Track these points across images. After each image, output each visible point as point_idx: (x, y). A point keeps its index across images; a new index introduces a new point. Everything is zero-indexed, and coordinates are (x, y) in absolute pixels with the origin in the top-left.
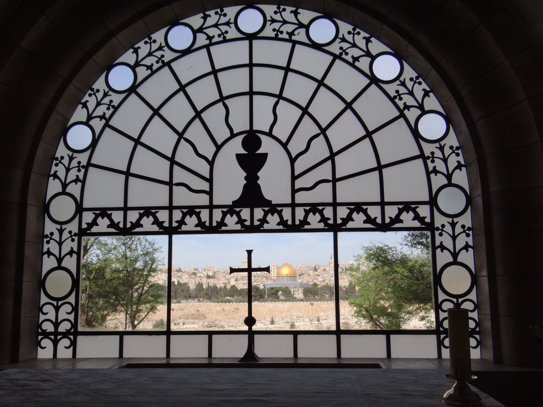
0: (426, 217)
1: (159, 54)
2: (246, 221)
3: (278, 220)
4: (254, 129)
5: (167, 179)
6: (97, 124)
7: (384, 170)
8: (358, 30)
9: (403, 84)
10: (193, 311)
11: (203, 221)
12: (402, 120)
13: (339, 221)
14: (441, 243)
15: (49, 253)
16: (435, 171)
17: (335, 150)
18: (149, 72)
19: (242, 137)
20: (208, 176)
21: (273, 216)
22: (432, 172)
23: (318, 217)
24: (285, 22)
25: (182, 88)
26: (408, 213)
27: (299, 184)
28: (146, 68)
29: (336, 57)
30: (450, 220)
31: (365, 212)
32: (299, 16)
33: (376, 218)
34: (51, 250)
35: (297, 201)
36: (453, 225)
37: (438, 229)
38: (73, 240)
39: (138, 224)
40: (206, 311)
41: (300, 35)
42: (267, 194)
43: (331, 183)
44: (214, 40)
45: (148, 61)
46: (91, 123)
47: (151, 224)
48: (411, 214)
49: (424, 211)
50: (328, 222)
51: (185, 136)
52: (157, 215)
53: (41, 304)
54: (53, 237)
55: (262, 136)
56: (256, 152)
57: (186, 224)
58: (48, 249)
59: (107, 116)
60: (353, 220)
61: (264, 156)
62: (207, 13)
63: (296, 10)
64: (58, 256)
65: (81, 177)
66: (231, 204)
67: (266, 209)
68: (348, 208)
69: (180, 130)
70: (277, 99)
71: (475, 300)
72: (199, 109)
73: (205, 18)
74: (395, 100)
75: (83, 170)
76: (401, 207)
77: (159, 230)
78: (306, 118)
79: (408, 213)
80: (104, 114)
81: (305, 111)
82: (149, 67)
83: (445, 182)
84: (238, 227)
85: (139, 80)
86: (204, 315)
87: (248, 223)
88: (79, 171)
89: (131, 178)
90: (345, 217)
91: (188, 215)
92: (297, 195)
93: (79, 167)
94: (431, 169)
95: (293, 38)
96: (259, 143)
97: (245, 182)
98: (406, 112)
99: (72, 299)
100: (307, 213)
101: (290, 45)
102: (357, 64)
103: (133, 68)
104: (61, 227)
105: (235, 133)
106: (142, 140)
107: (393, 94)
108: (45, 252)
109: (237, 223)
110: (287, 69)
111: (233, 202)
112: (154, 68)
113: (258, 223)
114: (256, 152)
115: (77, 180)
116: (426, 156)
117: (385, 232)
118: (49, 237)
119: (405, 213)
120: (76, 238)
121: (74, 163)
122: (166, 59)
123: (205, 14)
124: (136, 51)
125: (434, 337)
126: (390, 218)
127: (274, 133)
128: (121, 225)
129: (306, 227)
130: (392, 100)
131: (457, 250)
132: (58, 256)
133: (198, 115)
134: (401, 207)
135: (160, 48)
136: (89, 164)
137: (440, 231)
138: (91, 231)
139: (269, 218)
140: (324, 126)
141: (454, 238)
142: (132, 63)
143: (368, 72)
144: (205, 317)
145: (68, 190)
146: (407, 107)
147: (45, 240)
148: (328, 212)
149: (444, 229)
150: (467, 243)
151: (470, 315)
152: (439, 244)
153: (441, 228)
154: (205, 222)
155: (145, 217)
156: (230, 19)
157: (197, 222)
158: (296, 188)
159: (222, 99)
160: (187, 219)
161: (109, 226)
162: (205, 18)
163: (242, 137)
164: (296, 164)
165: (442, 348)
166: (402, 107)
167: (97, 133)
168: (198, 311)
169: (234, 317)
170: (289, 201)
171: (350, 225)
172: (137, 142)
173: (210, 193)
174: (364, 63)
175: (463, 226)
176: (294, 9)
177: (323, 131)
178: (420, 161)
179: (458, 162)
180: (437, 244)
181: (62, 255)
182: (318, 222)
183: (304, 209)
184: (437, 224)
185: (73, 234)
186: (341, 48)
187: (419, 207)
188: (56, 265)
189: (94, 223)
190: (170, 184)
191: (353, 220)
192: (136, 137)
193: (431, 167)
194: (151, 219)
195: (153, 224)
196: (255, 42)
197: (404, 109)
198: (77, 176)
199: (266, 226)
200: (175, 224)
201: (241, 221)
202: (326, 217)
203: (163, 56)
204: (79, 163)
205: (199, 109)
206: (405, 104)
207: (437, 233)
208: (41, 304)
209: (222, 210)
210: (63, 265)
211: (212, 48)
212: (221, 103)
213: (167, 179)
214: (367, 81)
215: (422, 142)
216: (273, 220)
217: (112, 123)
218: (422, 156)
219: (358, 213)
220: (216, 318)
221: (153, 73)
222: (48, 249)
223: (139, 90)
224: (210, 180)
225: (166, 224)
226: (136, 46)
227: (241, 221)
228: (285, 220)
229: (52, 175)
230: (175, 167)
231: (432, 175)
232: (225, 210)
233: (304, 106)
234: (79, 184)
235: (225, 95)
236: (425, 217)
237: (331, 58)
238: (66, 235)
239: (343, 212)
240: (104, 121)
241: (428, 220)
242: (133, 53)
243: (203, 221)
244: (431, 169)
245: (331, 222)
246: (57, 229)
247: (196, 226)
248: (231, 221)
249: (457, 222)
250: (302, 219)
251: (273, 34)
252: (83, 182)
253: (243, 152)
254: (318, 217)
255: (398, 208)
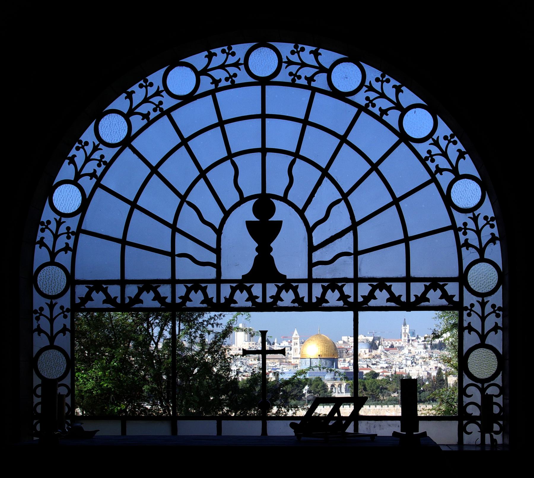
0: (454, 296)
1: (156, 100)
2: (257, 297)
3: (293, 297)
4: (267, 192)
5: (169, 250)
6: (87, 183)
7: (411, 243)
8: (387, 77)
9: (436, 143)
11: (210, 297)
12: (433, 185)
13: (360, 299)
14: (469, 324)
15: (40, 331)
16: (467, 245)
17: (357, 219)
18: (145, 121)
19: (253, 202)
20: (214, 246)
21: (287, 292)
22: (464, 245)
23: (337, 294)
24: (303, 65)
25: (184, 142)
26: (435, 291)
27: (317, 256)
28: (141, 117)
29: (361, 109)
30: (480, 299)
31: (389, 289)
32: (319, 57)
33: (401, 296)
34: (42, 327)
35: (314, 276)
36: (483, 305)
37: (466, 308)
38: (65, 317)
39: (137, 299)
41: (321, 82)
42: (282, 267)
43: (353, 256)
44: (220, 85)
45: (145, 108)
46: (81, 181)
47: (152, 300)
48: (439, 292)
49: (452, 289)
50: (348, 299)
51: (188, 199)
52: (159, 289)
53: (34, 386)
54: (43, 313)
55: (276, 202)
56: (269, 220)
57: (190, 300)
58: (39, 326)
59: (98, 174)
60: (375, 298)
61: (279, 224)
62: (213, 51)
63: (317, 50)
64: (49, 332)
65: (71, 245)
66: (241, 278)
67: (280, 285)
68: (369, 285)
69: (183, 193)
70: (292, 158)
71: (501, 385)
72: (204, 168)
73: (210, 56)
74: (427, 162)
75: (73, 237)
76: (428, 284)
77: (161, 306)
78: (326, 180)
79: (435, 291)
80: (95, 171)
81: (325, 173)
82: (145, 116)
83: (477, 256)
84: (249, 304)
85: (134, 132)
87: (260, 300)
88: (69, 238)
89: (127, 248)
90: (367, 295)
91: (193, 291)
92: (314, 269)
93: (68, 233)
94: (462, 241)
95: (313, 84)
96: (272, 210)
97: (257, 254)
98: (438, 176)
99: (67, 381)
100: (325, 290)
101: (309, 92)
102: (385, 117)
103: (127, 117)
104: (51, 302)
105: (245, 196)
106: (139, 203)
107: (424, 155)
108: (35, 329)
109: (247, 300)
110: (305, 122)
111: (243, 276)
112: (151, 117)
113: (272, 300)
114: (269, 220)
115: (66, 249)
116: (458, 227)
117: (410, 311)
118: (39, 313)
119: (432, 291)
120: (69, 314)
121: (63, 229)
122: (165, 107)
123: (210, 53)
124: (130, 96)
125: (455, 424)
126: (416, 296)
127: (290, 198)
128: (119, 301)
129: (324, 305)
130: (423, 161)
131: (486, 331)
132: (49, 332)
133: (203, 174)
134: (428, 284)
135: (158, 93)
136: (80, 230)
137: (469, 311)
138: (85, 306)
139: (283, 294)
140: (345, 190)
141: (483, 318)
142: (125, 111)
143: (396, 127)
145: (57, 260)
146: (440, 170)
147: (35, 316)
148: (348, 289)
149: (473, 309)
150: (496, 323)
151: (495, 400)
152: (467, 325)
153: (469, 308)
154: (213, 297)
155: (145, 293)
156: (239, 59)
157: (203, 298)
158: (314, 260)
159: (230, 156)
160: (192, 295)
161: (104, 302)
162: (210, 56)
163: (253, 202)
164: (313, 234)
165: (464, 434)
166: (433, 169)
167: (88, 194)
170: (305, 276)
171: (372, 303)
172: (134, 205)
173: (218, 266)
174: (393, 117)
175: (493, 306)
176: (314, 48)
177: (345, 196)
178: (451, 233)
179: (493, 234)
180: (465, 324)
181: (54, 333)
182: (337, 300)
183: (322, 285)
184: (466, 303)
185: (65, 310)
186: (367, 98)
187: (447, 284)
188: (48, 343)
189: (88, 297)
190: (172, 254)
191: (375, 298)
192: (132, 199)
193: (462, 239)
194: (152, 294)
195: (154, 299)
196: (268, 88)
197: (436, 172)
198: (67, 244)
199: (280, 303)
200: (178, 301)
201: (252, 298)
202: (346, 294)
203: (161, 103)
204: (68, 228)
205: (204, 168)
206: (437, 166)
207: (465, 313)
208: (34, 386)
209: (230, 286)
210: (56, 343)
211: (218, 95)
212: (229, 162)
213: (169, 250)
214: (396, 139)
215: (454, 212)
216: (288, 297)
217: (102, 182)
218: (453, 227)
219: (381, 291)
221: (150, 123)
222: (39, 326)
223: (133, 143)
224: (217, 251)
225: (169, 300)
226: (129, 90)
227: (252, 298)
228: (300, 297)
229: (38, 243)
230: (178, 235)
231: (464, 249)
232: (234, 285)
233: (324, 166)
234: (70, 253)
235: (233, 151)
236: (454, 296)
237: (355, 110)
238: (57, 310)
239: (364, 289)
240: (94, 180)
241: (456, 299)
242: (126, 98)
243: (210, 297)
244: (462, 241)
245: (351, 300)
246: (47, 304)
247: (202, 302)
248: (241, 298)
249: (488, 301)
250: (319, 297)
251: (289, 79)
252: (74, 251)
253: (254, 219)
254: (337, 294)
255: (425, 285)
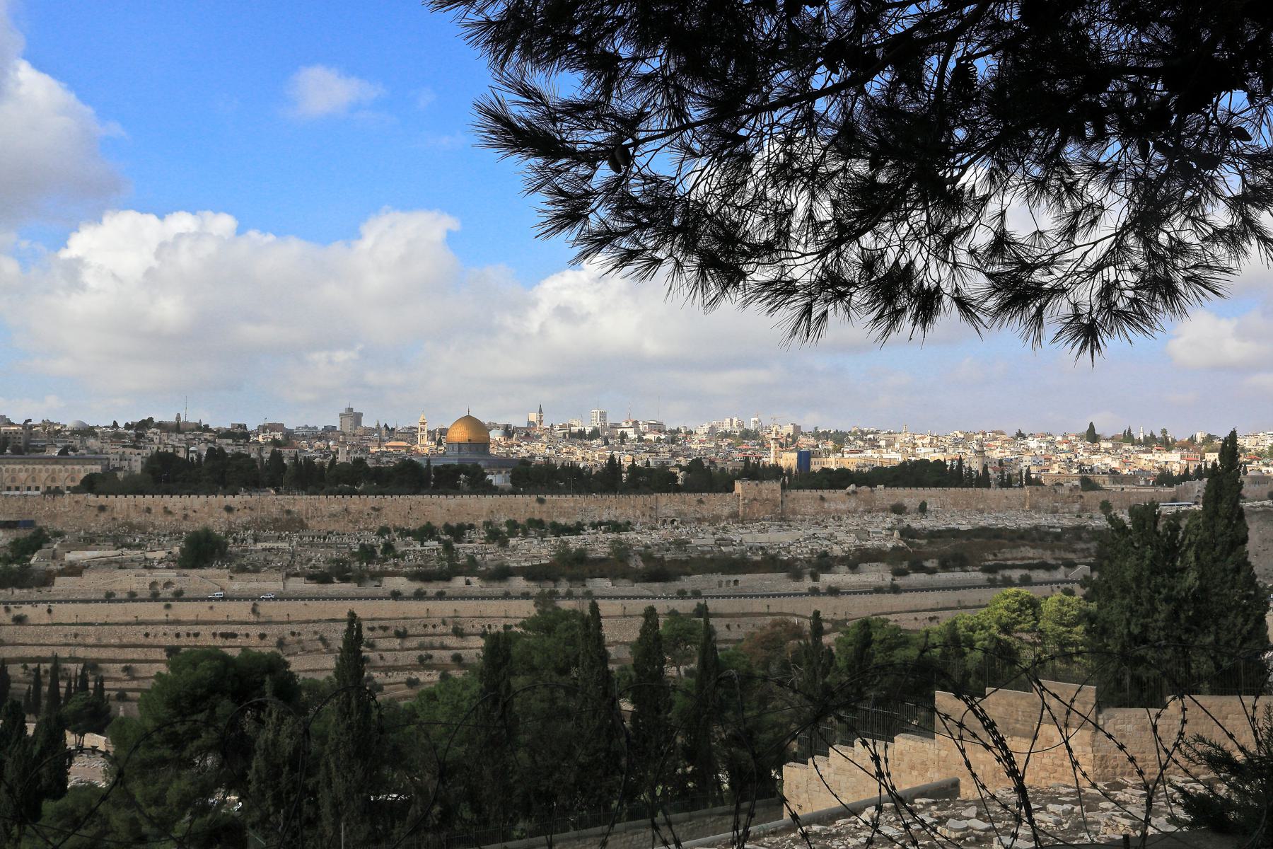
10: (275, 511)
40: (307, 513)
86: (301, 521)
144: (303, 526)
168: (289, 512)
169: (371, 527)
220: (330, 529)
